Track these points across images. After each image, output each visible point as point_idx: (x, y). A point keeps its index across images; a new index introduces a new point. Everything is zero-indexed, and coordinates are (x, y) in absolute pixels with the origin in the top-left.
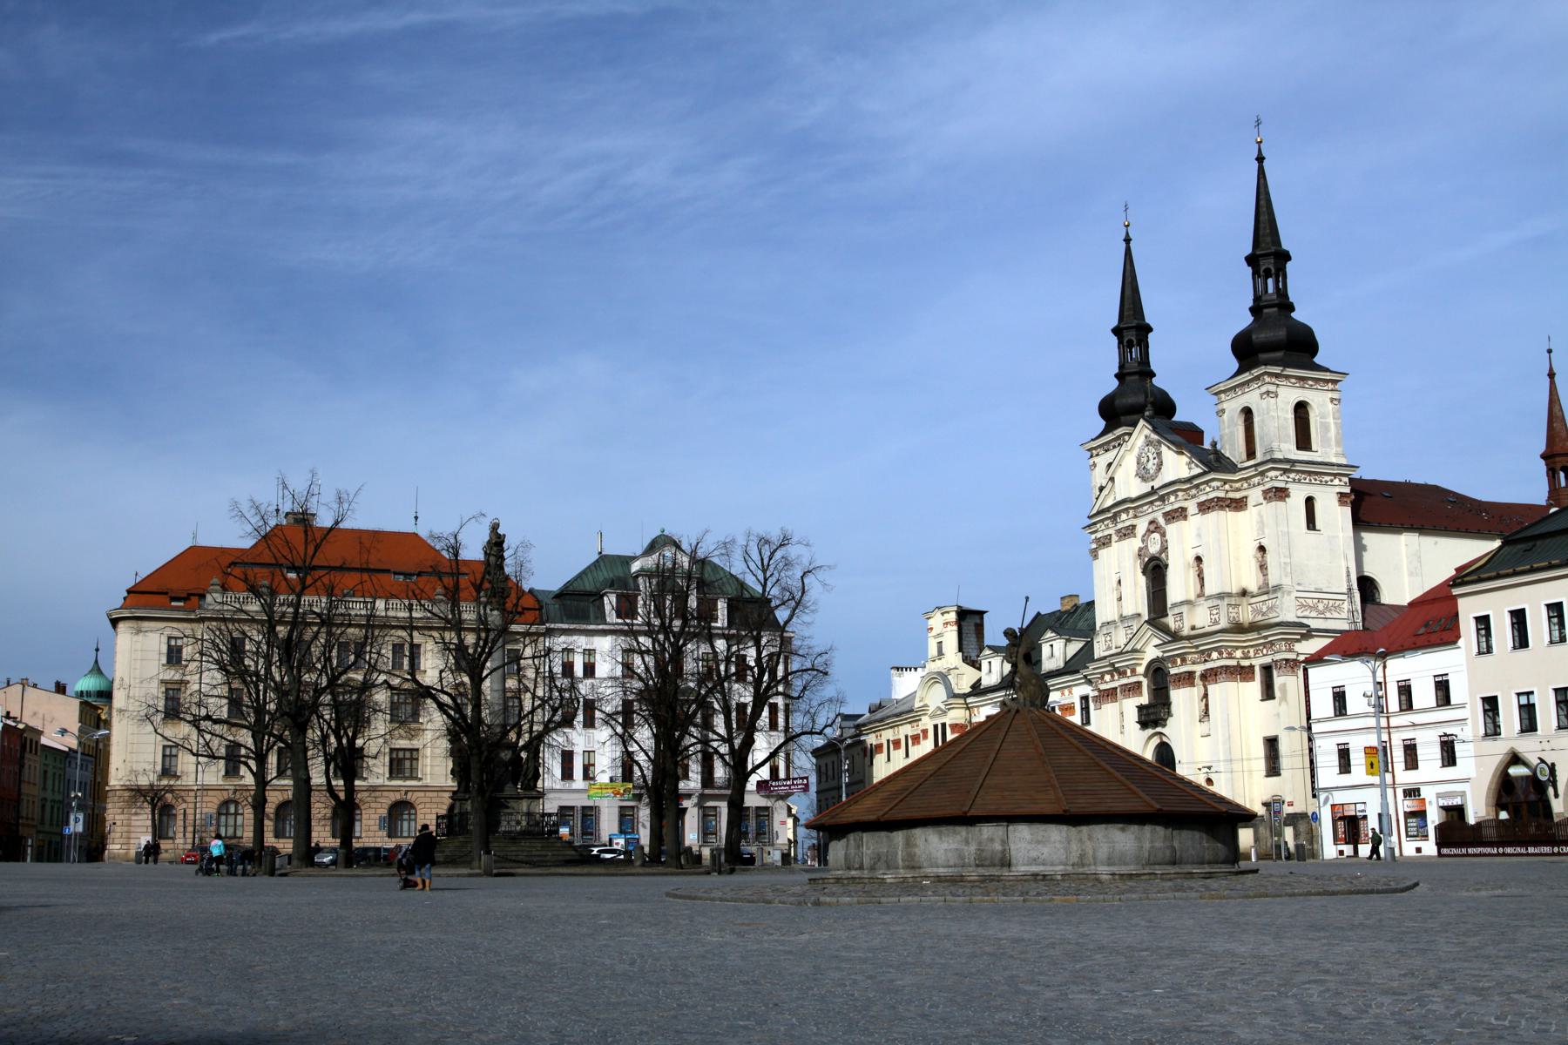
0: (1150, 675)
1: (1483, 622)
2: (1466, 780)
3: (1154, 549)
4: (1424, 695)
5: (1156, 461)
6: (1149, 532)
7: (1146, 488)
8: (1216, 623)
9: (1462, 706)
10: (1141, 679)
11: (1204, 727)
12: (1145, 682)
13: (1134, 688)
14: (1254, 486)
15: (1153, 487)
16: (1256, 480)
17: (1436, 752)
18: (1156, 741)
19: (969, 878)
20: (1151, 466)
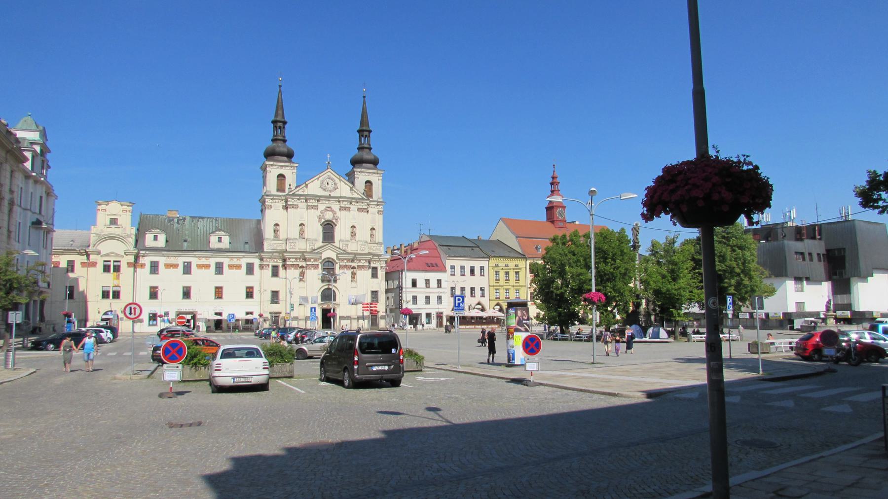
0: (323, 264)
1: (453, 267)
2: (444, 308)
3: (329, 216)
4: (433, 284)
5: (333, 186)
6: (326, 210)
7: (327, 194)
8: (363, 250)
9: (445, 288)
10: (319, 264)
11: (354, 284)
12: (320, 266)
13: (316, 267)
14: (372, 207)
15: (330, 195)
16: (373, 206)
17: (424, 300)
18: (327, 287)
19: (137, 337)
20: (330, 187)
